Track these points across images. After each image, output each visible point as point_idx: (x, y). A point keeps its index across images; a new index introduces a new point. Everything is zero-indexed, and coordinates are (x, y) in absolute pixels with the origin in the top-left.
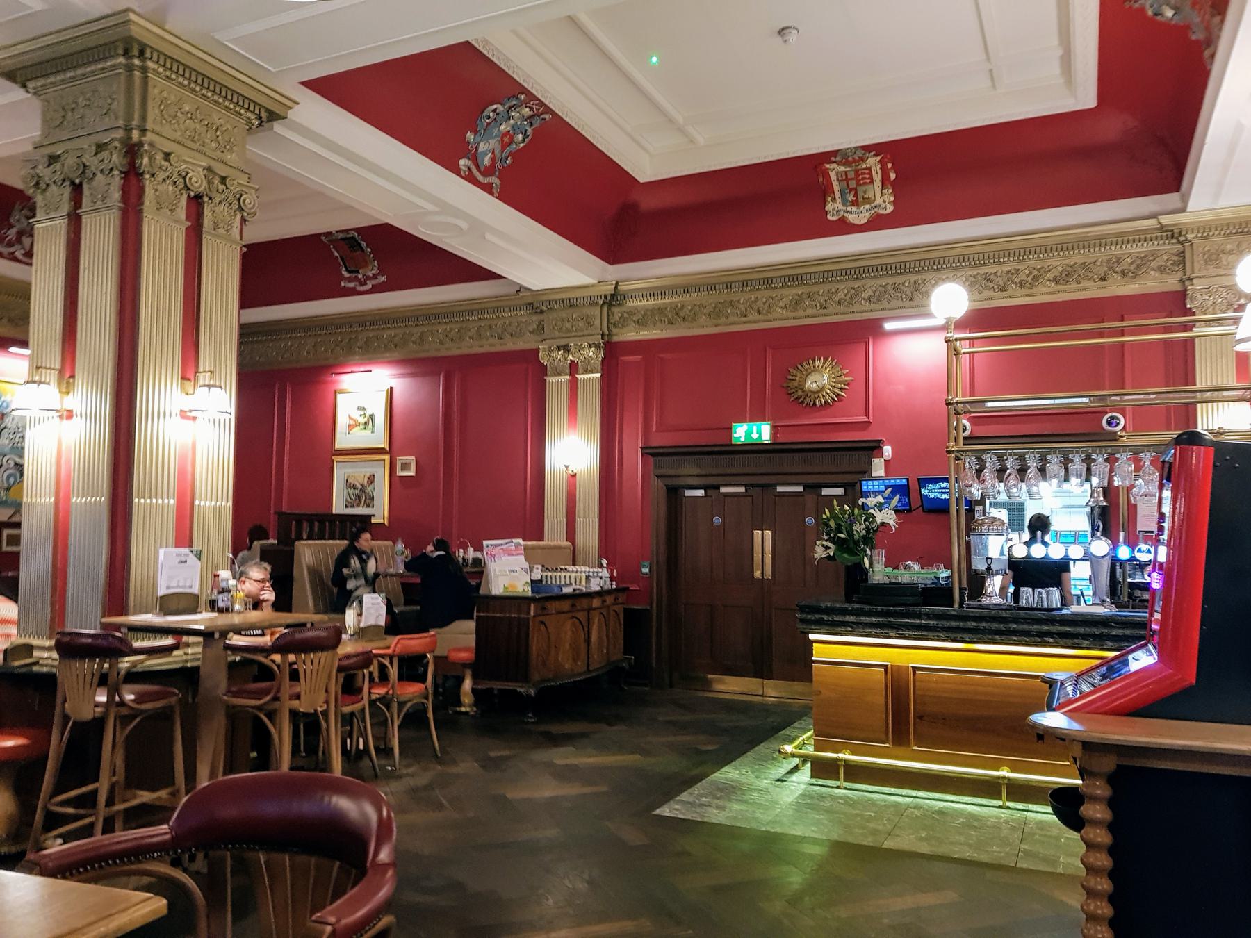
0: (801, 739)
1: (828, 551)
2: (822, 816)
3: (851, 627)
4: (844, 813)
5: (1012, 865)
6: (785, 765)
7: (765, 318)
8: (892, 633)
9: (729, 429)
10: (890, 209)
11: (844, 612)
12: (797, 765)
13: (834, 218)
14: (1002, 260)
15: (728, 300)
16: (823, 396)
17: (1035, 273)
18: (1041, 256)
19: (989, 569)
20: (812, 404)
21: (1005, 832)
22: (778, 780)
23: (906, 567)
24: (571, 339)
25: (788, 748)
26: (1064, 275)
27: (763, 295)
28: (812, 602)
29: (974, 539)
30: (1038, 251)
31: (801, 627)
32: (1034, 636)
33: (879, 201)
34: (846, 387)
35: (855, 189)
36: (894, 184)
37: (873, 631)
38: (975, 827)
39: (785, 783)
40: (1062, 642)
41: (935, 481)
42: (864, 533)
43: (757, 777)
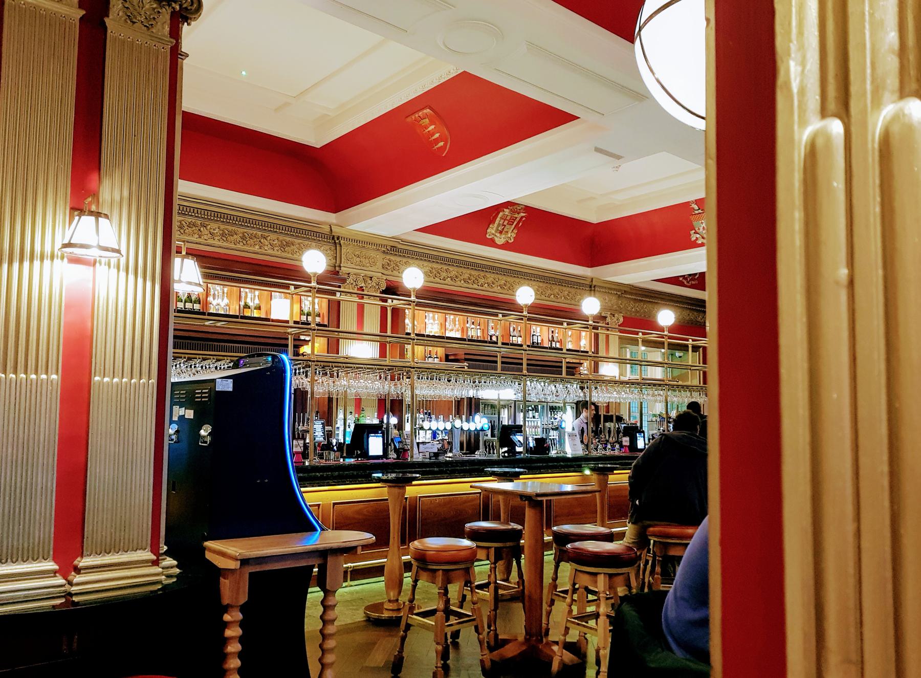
13: (490, 237)
33: (509, 235)
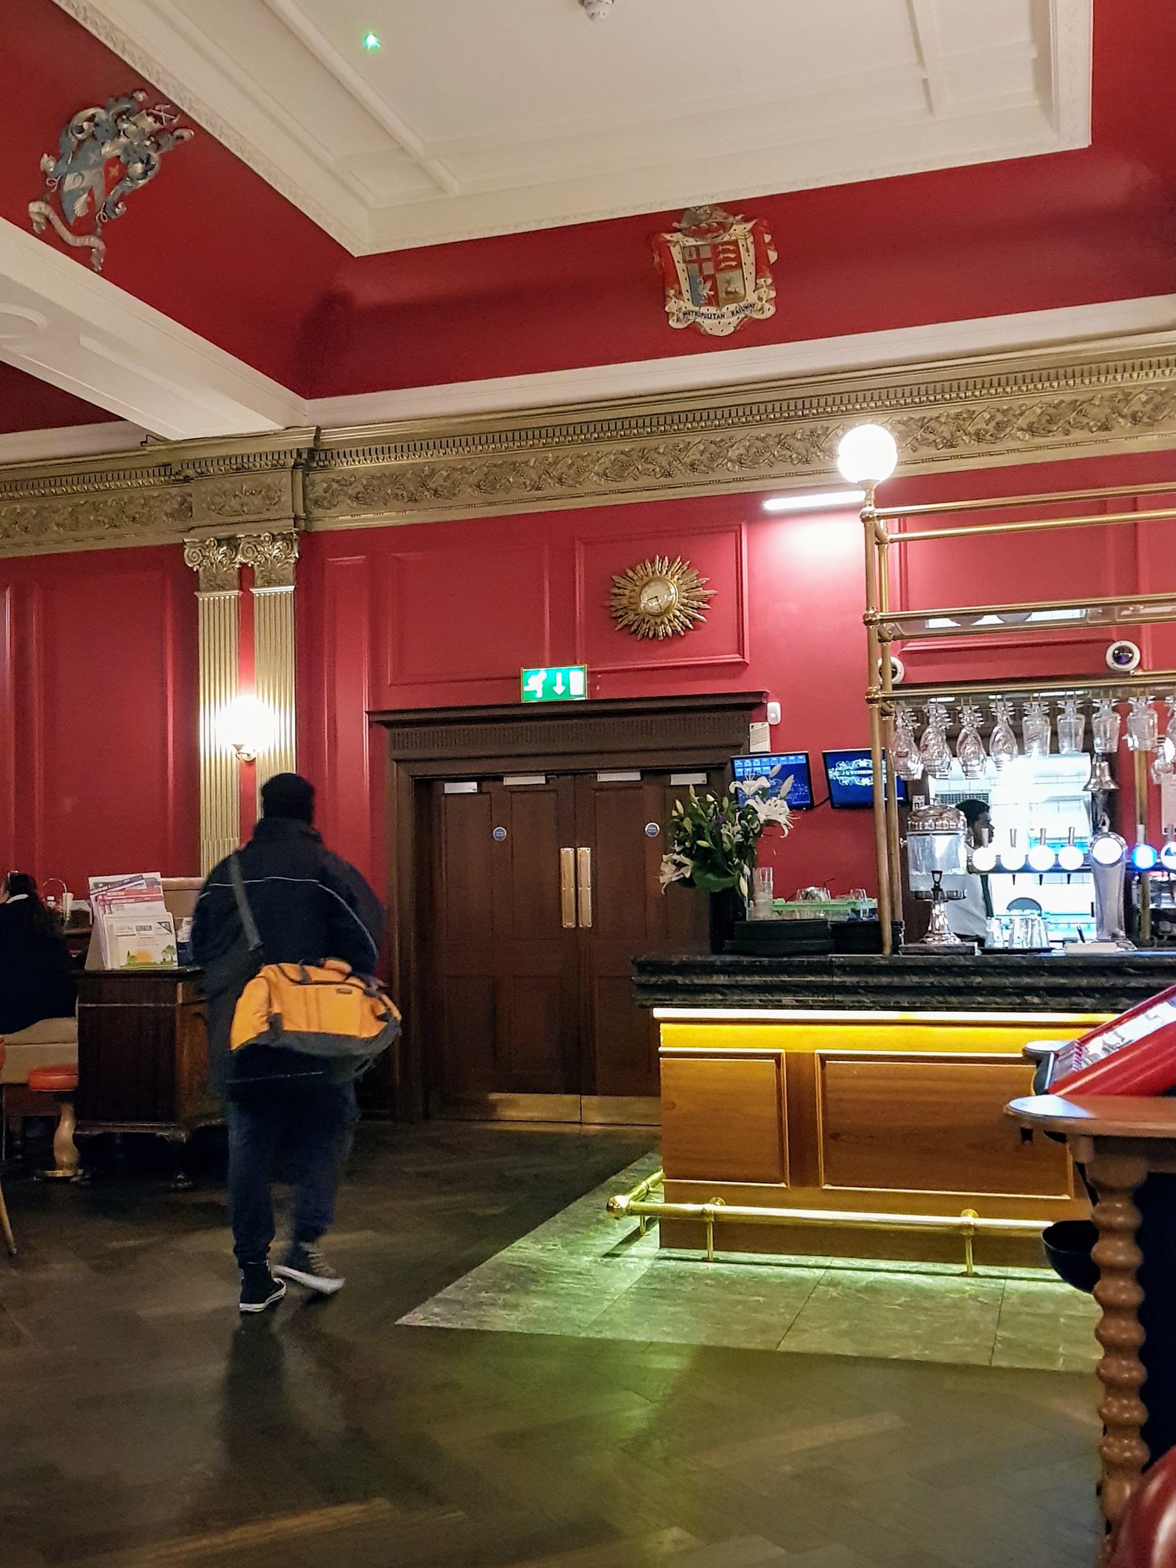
0: (643, 1185)
1: (682, 870)
2: (678, 1309)
3: (722, 994)
4: (716, 1301)
5: (986, 1363)
6: (618, 1230)
7: (571, 491)
8: (787, 999)
9: (517, 679)
10: (770, 310)
11: (710, 969)
12: (639, 1228)
14: (947, 396)
15: (510, 460)
16: (670, 621)
17: (999, 417)
18: (1008, 389)
19: (937, 889)
20: (651, 635)
21: (972, 1314)
22: (607, 1255)
23: (807, 896)
24: (243, 526)
25: (622, 1201)
26: (1044, 421)
27: (568, 453)
28: (653, 955)
29: (912, 842)
30: (1003, 382)
31: (641, 997)
32: (1009, 994)
33: (752, 297)
34: (707, 606)
35: (712, 277)
36: (774, 269)
37: (756, 998)
38: (926, 1309)
39: (617, 1259)
40: (1053, 1001)
41: (849, 757)
42: (739, 838)
43: (571, 1253)
